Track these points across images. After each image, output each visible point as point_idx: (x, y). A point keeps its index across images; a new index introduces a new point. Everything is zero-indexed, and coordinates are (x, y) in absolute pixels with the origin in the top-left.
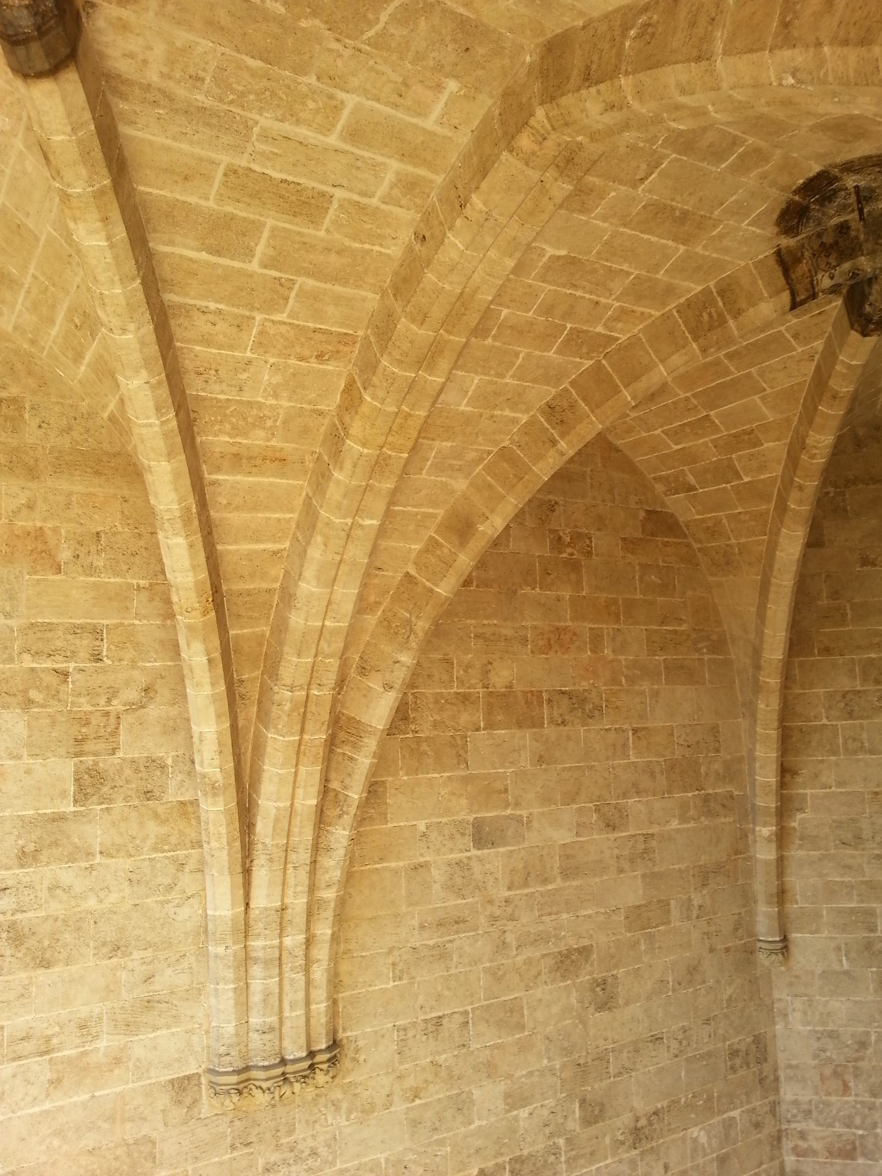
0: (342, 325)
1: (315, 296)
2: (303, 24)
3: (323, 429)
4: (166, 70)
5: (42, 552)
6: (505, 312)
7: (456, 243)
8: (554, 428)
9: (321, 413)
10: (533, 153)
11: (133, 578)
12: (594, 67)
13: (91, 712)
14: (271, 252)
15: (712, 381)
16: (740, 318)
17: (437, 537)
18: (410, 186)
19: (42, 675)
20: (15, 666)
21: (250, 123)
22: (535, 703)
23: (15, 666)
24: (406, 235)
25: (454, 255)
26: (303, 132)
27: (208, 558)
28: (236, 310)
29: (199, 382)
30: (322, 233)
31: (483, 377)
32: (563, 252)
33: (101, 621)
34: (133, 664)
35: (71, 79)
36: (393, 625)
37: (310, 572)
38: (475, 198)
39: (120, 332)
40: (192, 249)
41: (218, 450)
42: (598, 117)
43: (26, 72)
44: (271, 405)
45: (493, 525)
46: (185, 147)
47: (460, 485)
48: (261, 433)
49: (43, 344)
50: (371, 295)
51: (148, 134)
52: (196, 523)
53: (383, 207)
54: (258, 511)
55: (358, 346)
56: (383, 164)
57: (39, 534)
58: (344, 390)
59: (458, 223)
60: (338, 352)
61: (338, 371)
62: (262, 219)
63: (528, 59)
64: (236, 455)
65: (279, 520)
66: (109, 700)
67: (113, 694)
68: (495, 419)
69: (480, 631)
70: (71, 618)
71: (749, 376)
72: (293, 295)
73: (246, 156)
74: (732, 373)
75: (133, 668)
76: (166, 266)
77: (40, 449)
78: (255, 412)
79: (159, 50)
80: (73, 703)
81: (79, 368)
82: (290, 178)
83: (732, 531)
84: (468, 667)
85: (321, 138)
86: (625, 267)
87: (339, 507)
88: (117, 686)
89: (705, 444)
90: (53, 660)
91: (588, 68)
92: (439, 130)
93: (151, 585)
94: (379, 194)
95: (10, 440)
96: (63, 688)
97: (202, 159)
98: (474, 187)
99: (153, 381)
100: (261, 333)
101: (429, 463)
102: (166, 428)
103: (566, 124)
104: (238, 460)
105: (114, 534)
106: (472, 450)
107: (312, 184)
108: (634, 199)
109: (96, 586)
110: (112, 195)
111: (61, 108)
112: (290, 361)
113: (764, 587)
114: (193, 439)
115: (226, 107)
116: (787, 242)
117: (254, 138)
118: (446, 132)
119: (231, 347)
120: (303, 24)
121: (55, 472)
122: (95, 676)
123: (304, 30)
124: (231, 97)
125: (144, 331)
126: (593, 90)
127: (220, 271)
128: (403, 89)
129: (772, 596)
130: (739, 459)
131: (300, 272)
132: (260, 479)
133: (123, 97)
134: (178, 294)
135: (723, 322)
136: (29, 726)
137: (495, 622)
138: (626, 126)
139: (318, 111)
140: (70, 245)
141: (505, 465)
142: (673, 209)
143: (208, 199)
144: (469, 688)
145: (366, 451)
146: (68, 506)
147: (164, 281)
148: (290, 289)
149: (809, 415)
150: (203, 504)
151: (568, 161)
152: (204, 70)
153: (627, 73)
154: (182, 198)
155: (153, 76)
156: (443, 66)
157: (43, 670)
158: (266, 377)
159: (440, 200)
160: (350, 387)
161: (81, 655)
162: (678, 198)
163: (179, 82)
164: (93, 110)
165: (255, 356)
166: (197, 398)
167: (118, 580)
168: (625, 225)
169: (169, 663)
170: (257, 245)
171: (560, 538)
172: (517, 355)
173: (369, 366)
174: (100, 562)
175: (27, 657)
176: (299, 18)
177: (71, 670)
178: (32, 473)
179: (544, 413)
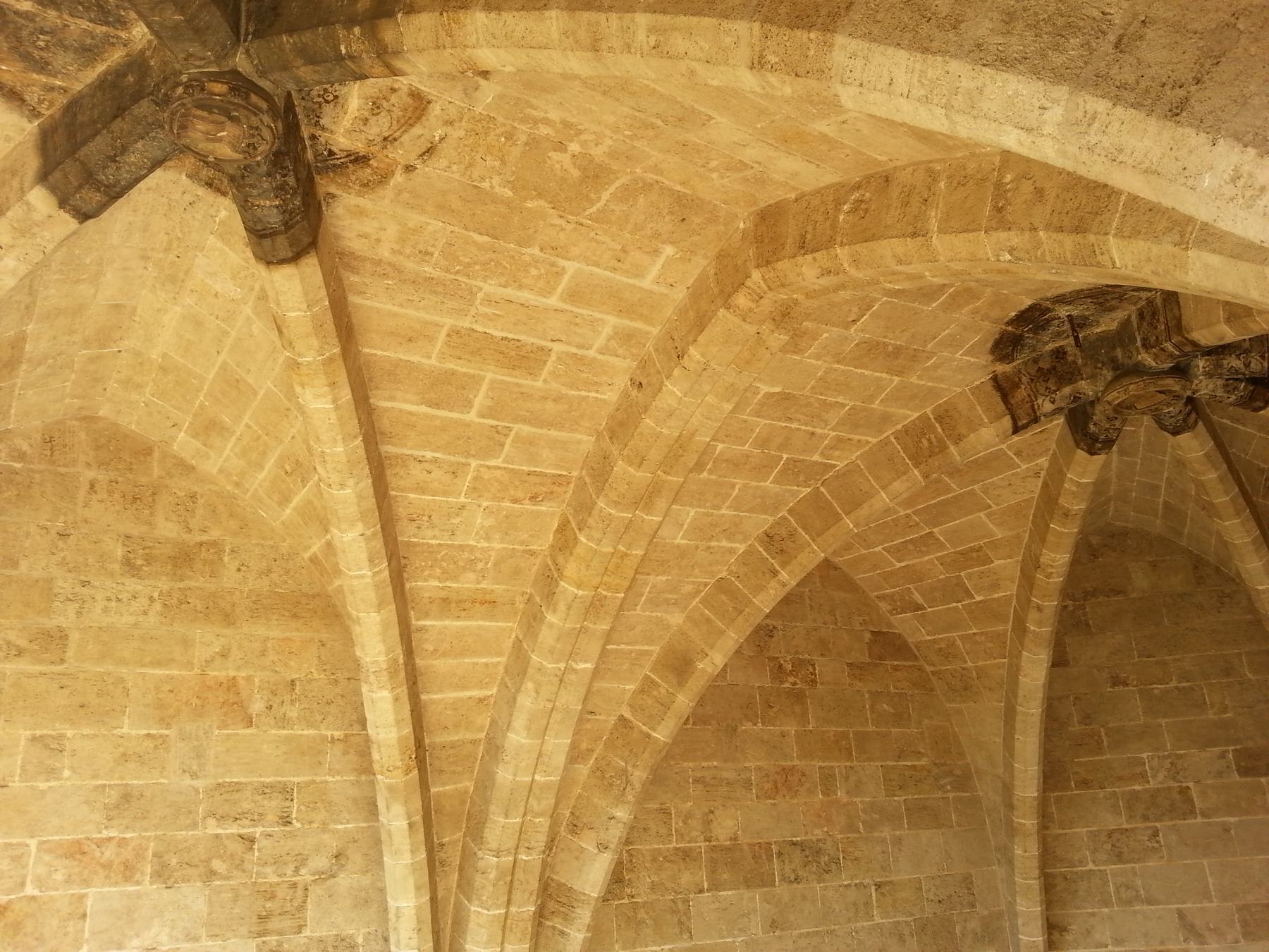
0: (558, 467)
1: (531, 441)
2: (529, 204)
3: (535, 569)
4: (396, 247)
6: (720, 446)
7: (673, 391)
9: (532, 553)
10: (750, 310)
11: (327, 729)
12: (809, 237)
13: (278, 884)
14: (489, 403)
15: (933, 498)
16: (962, 444)
18: (626, 338)
19: (227, 842)
20: (199, 833)
21: (475, 289)
23: (199, 833)
24: (622, 382)
25: (673, 402)
26: (525, 296)
27: (412, 711)
28: (452, 458)
29: (412, 528)
30: (539, 384)
32: (777, 390)
35: (311, 264)
37: (519, 721)
38: (693, 350)
40: (412, 403)
41: (427, 595)
42: (815, 280)
43: (270, 260)
44: (483, 548)
45: (713, 661)
46: (411, 312)
47: (676, 619)
48: (471, 576)
50: (585, 438)
51: (374, 302)
52: (403, 674)
53: (600, 357)
54: (466, 659)
55: (572, 486)
56: (602, 320)
57: (232, 684)
58: (557, 530)
59: (676, 372)
60: (552, 493)
61: (552, 513)
63: (742, 225)
64: (444, 600)
65: (487, 665)
66: (297, 870)
67: (302, 861)
69: (699, 775)
71: (972, 493)
72: (509, 441)
73: (469, 318)
74: (954, 490)
75: (324, 831)
76: (385, 420)
77: (237, 592)
78: (466, 555)
79: (392, 230)
80: (257, 874)
82: (511, 336)
84: (687, 817)
85: (544, 300)
86: (840, 399)
87: (552, 652)
91: (803, 236)
92: (655, 288)
93: (346, 736)
94: (595, 347)
95: (207, 585)
97: (426, 323)
98: (691, 339)
99: (368, 533)
100: (475, 479)
102: (377, 579)
103: (783, 286)
104: (447, 605)
106: (688, 583)
108: (846, 338)
109: (288, 739)
110: (341, 362)
111: (299, 288)
113: (1010, 715)
114: (403, 585)
116: (1002, 368)
117: (478, 302)
118: (663, 290)
119: (445, 493)
120: (529, 204)
122: (282, 842)
123: (527, 208)
125: (362, 485)
126: (809, 257)
127: (438, 423)
128: (622, 255)
129: (1019, 726)
132: (469, 623)
133: (355, 271)
134: (395, 445)
135: (943, 448)
136: (210, 903)
138: (843, 286)
139: (539, 277)
140: (289, 400)
141: (723, 597)
142: (886, 345)
143: (430, 358)
144: (689, 842)
145: (580, 593)
146: (263, 653)
147: (383, 434)
148: (506, 435)
149: (1040, 532)
150: (409, 652)
151: (784, 316)
152: (433, 246)
153: (842, 244)
154: (406, 358)
155: (384, 252)
156: (660, 235)
157: (228, 837)
159: (656, 350)
160: (563, 527)
162: (890, 335)
163: (409, 257)
164: (327, 286)
166: (409, 545)
167: (312, 732)
168: (838, 362)
171: (781, 666)
172: (733, 486)
173: (584, 508)
174: (293, 713)
175: (212, 822)
176: (526, 200)
178: (228, 619)
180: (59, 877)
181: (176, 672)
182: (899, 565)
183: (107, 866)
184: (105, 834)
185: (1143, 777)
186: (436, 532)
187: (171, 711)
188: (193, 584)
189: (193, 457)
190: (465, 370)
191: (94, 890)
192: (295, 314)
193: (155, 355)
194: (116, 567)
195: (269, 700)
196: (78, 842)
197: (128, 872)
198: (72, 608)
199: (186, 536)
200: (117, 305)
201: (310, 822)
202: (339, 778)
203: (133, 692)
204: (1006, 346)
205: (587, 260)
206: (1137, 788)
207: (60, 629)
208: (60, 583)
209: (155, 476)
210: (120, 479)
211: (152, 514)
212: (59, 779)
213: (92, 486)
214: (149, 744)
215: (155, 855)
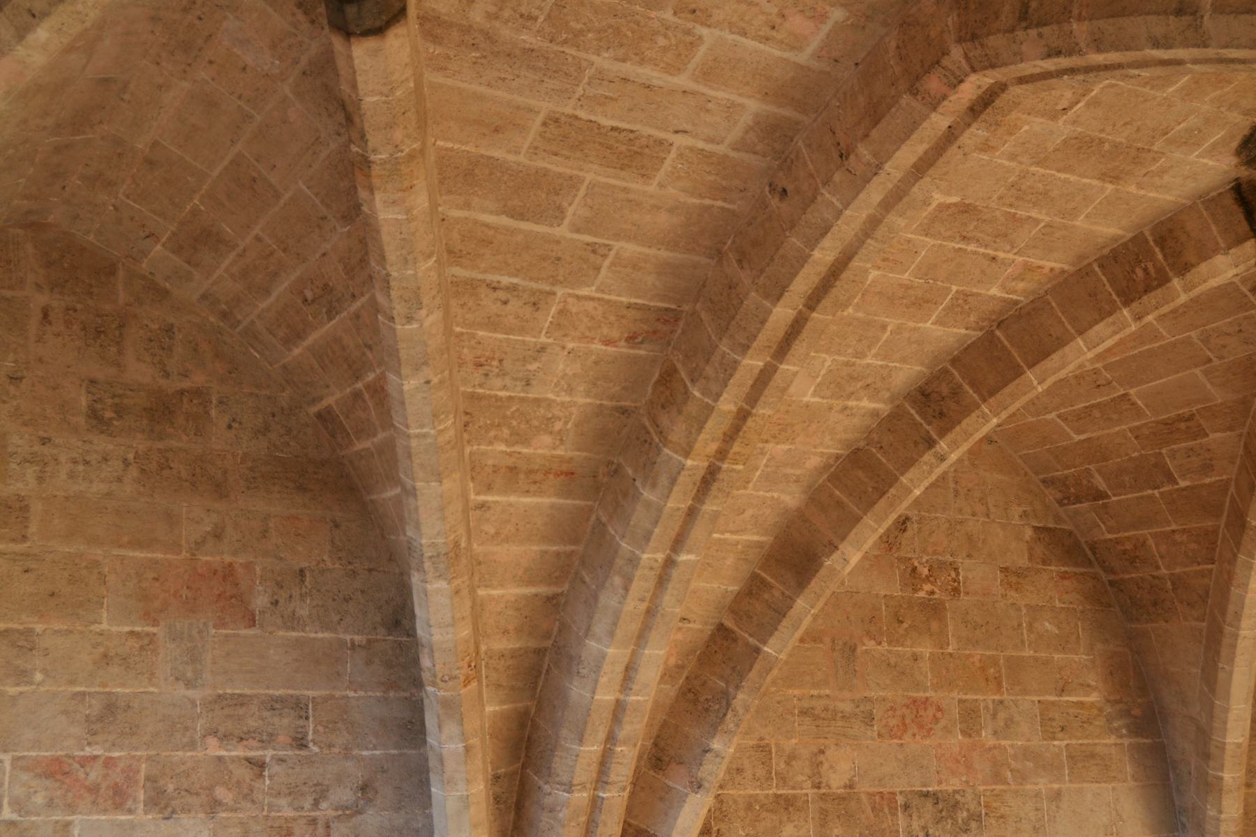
4: (491, 9)
5: (231, 597)
8: (929, 423)
11: (346, 631)
13: (294, 819)
17: (764, 575)
19: (231, 767)
20: (200, 754)
21: (584, 64)
22: (886, 810)
23: (200, 754)
26: (648, 73)
28: (534, 285)
30: (652, 188)
31: (837, 357)
33: (306, 692)
34: (347, 752)
36: (702, 699)
39: (404, 321)
40: (491, 213)
41: (490, 462)
44: (563, 403)
46: (500, 94)
48: (547, 439)
49: (239, 317)
57: (228, 573)
58: (658, 382)
59: (837, 177)
62: (581, 174)
64: (512, 469)
66: (316, 804)
67: (321, 794)
68: (848, 412)
69: (806, 704)
70: (268, 688)
72: (607, 263)
73: (573, 102)
75: (346, 757)
80: (271, 806)
81: (290, 350)
83: (1162, 557)
84: (791, 758)
85: (670, 78)
88: (326, 782)
90: (246, 746)
93: (369, 641)
96: (257, 785)
100: (561, 312)
101: (758, 473)
105: (322, 572)
106: (815, 454)
107: (648, 131)
109: (299, 643)
112: (593, 346)
115: (556, 48)
119: (522, 330)
121: (248, 488)
122: (298, 769)
124: (564, 36)
127: (520, 238)
131: (617, 236)
137: (828, 692)
141: (860, 473)
144: (793, 788)
146: (264, 534)
148: (605, 256)
157: (233, 759)
158: (561, 367)
161: (281, 738)
165: (551, 340)
167: (327, 635)
169: (393, 752)
170: (570, 205)
171: (914, 569)
172: (884, 327)
174: (304, 611)
175: (212, 741)
177: (268, 760)
179: (914, 402)
180: (39, 799)
181: (160, 556)
182: (1077, 438)
183: (94, 789)
184: (88, 751)
186: (508, 381)
187: (157, 604)
188: (174, 443)
189: (167, 278)
190: (560, 170)
191: (80, 817)
192: (375, 99)
193: (141, 144)
194: (81, 420)
195: (274, 593)
196: (57, 760)
197: (119, 798)
198: (31, 472)
199: (163, 382)
200: (106, 80)
201: (330, 746)
202: (362, 693)
203: (111, 579)
205: (732, 27)
207: (20, 498)
208: (15, 439)
209: (121, 302)
210: (79, 306)
211: (120, 352)
212: (31, 683)
213: (45, 314)
214: (133, 643)
215: (148, 779)
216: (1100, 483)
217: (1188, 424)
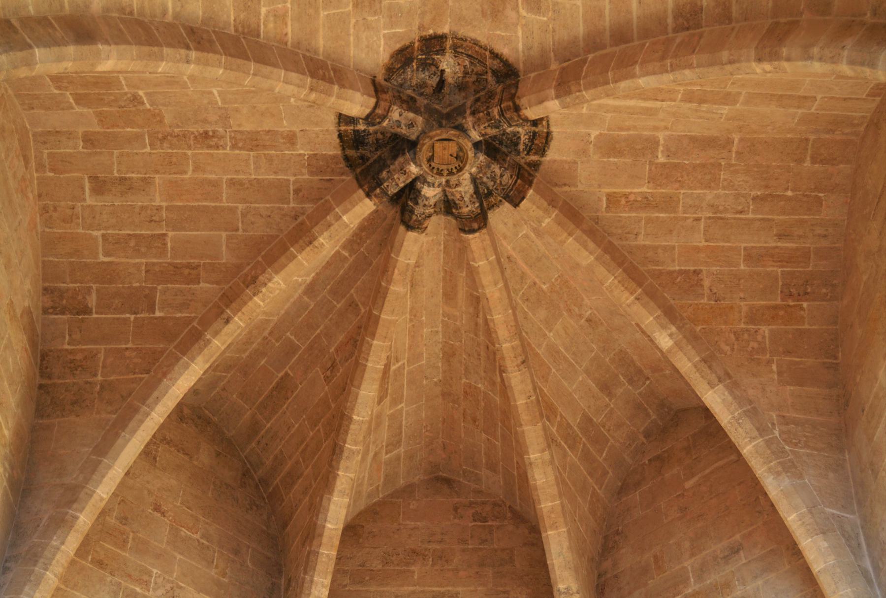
74: (221, 201)
83: (104, 367)
89: (137, 266)
130: (164, 292)
182: (102, 258)
185: (147, 584)
204: (403, 57)
206: (138, 590)
216: (92, 301)
217: (194, 272)
